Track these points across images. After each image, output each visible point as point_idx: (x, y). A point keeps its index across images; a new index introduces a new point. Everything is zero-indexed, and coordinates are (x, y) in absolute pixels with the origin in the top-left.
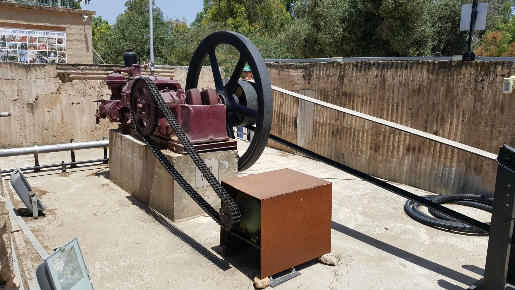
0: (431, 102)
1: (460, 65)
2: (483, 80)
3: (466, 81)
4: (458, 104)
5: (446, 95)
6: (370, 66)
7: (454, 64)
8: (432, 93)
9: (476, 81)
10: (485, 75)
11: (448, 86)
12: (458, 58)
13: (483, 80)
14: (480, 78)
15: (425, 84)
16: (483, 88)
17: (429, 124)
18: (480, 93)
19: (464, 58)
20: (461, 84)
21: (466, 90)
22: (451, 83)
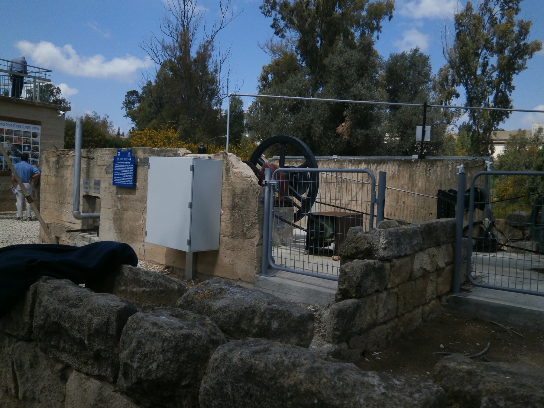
0: (400, 184)
1: (416, 161)
2: (430, 170)
3: (421, 170)
4: (416, 184)
5: (410, 179)
6: (360, 162)
7: (413, 161)
8: (401, 178)
9: (426, 170)
10: (431, 166)
11: (410, 174)
12: (415, 157)
13: (430, 170)
14: (428, 169)
15: (396, 173)
16: (430, 174)
17: (400, 197)
18: (429, 177)
19: (419, 157)
20: (417, 173)
21: (420, 176)
22: (412, 172)
